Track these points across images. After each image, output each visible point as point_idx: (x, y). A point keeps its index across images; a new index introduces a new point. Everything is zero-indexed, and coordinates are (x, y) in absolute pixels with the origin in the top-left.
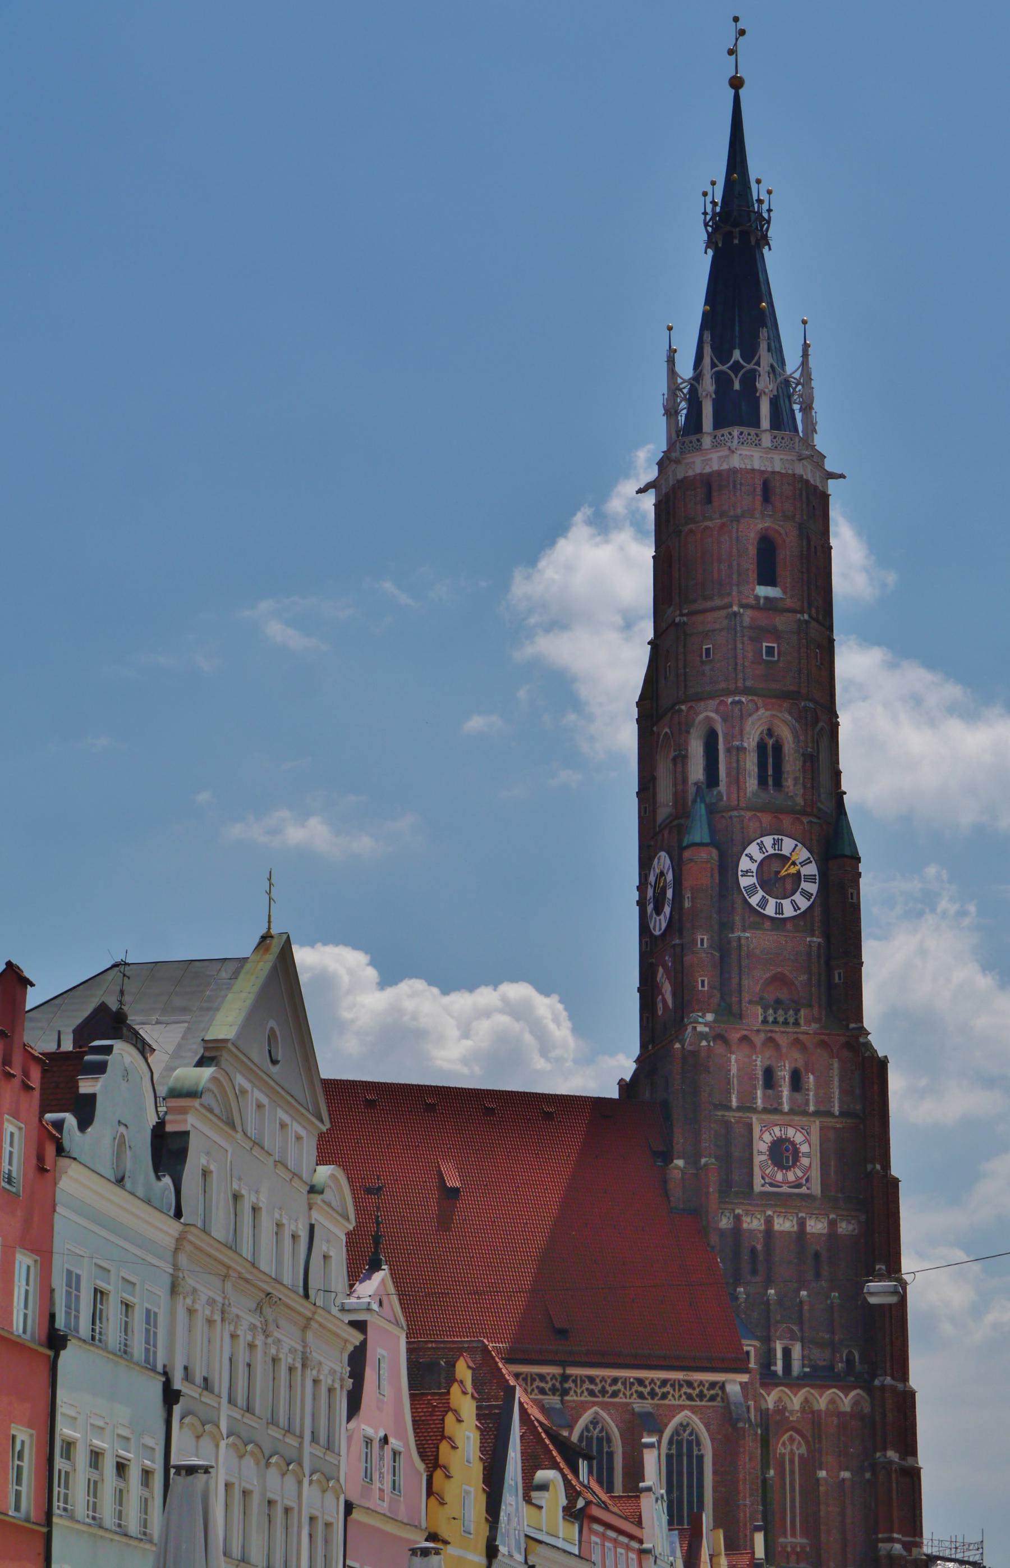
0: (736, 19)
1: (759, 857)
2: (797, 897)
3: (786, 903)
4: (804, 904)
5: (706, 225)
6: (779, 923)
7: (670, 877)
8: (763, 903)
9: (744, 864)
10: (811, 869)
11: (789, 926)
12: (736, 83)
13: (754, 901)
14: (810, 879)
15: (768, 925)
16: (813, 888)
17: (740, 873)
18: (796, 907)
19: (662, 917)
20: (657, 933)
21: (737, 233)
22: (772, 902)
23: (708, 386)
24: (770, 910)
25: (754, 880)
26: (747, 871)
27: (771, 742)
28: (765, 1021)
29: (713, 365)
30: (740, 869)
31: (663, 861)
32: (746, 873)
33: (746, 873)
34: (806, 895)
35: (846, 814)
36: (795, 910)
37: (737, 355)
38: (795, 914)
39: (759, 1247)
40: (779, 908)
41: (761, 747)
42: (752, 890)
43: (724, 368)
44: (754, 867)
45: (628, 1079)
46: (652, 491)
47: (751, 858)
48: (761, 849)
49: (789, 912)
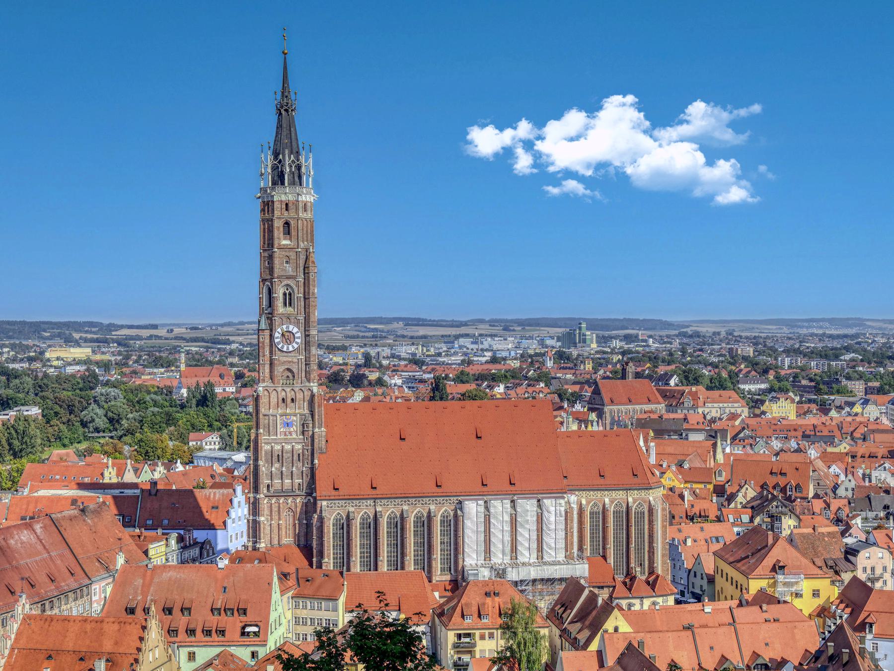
4: (296, 346)
9: (277, 335)
13: (280, 346)
24: (285, 349)
40: (288, 348)
42: (279, 343)
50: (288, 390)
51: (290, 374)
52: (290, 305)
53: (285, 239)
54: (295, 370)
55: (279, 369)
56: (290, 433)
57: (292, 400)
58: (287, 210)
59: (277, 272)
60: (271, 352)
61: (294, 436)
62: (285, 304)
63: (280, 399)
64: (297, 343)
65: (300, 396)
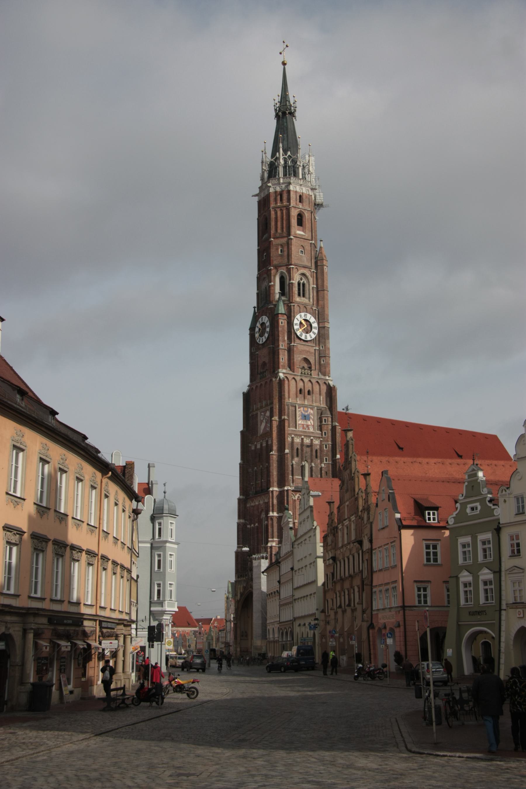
0: (284, 42)
2: (311, 333)
3: (308, 335)
4: (313, 336)
5: (276, 110)
7: (268, 324)
9: (296, 321)
10: (315, 325)
12: (284, 64)
13: (298, 333)
14: (315, 328)
15: (302, 342)
16: (316, 331)
18: (311, 337)
19: (264, 337)
20: (261, 343)
21: (284, 113)
22: (304, 335)
23: (282, 162)
24: (303, 337)
27: (302, 282)
28: (302, 373)
29: (283, 155)
31: (265, 319)
32: (296, 324)
34: (314, 333)
37: (289, 153)
39: (299, 448)
40: (306, 337)
41: (299, 284)
43: (286, 157)
46: (257, 197)
49: (309, 338)
50: (306, 380)
51: (306, 366)
52: (304, 296)
53: (299, 230)
54: (312, 361)
55: (298, 358)
56: (308, 426)
57: (309, 392)
58: (300, 202)
59: (294, 260)
60: (289, 338)
61: (311, 430)
62: (299, 295)
63: (298, 389)
65: (316, 388)
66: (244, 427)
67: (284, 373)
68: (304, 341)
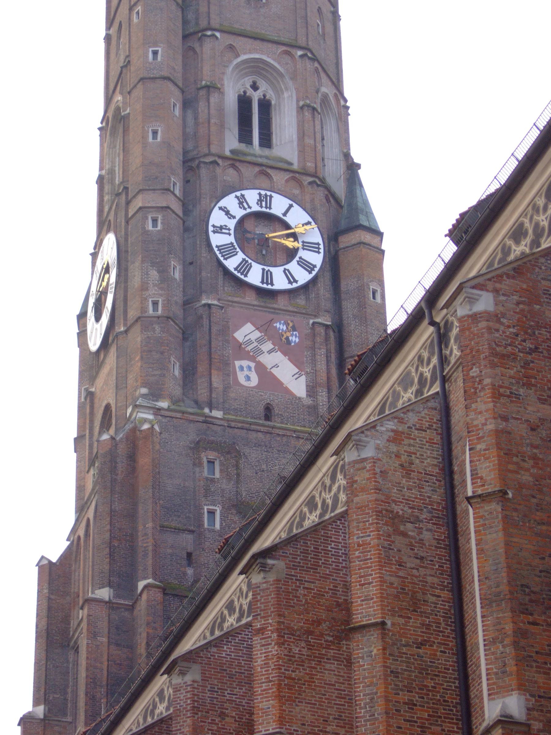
1: (239, 213)
2: (293, 266)
4: (303, 277)
6: (267, 294)
8: (244, 267)
9: (217, 218)
11: (282, 302)
13: (231, 264)
15: (250, 298)
16: (317, 259)
17: (211, 229)
18: (291, 279)
25: (231, 239)
26: (221, 228)
27: (256, 96)
30: (211, 223)
32: (220, 230)
33: (220, 230)
34: (307, 266)
35: (361, 185)
36: (290, 282)
38: (289, 287)
40: (267, 277)
44: (232, 224)
45: (54, 559)
47: (227, 213)
48: (241, 203)
49: (280, 282)
64: (307, 266)
66: (36, 703)
67: (157, 411)
68: (259, 291)
